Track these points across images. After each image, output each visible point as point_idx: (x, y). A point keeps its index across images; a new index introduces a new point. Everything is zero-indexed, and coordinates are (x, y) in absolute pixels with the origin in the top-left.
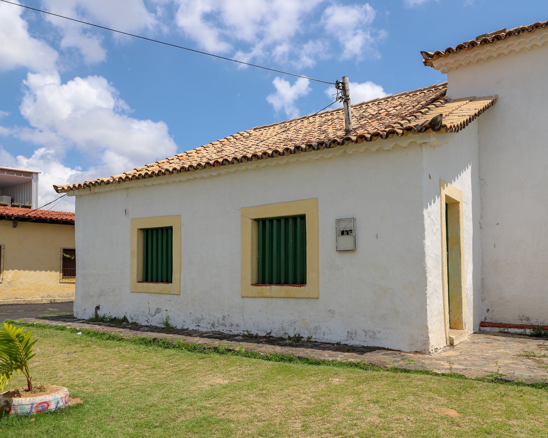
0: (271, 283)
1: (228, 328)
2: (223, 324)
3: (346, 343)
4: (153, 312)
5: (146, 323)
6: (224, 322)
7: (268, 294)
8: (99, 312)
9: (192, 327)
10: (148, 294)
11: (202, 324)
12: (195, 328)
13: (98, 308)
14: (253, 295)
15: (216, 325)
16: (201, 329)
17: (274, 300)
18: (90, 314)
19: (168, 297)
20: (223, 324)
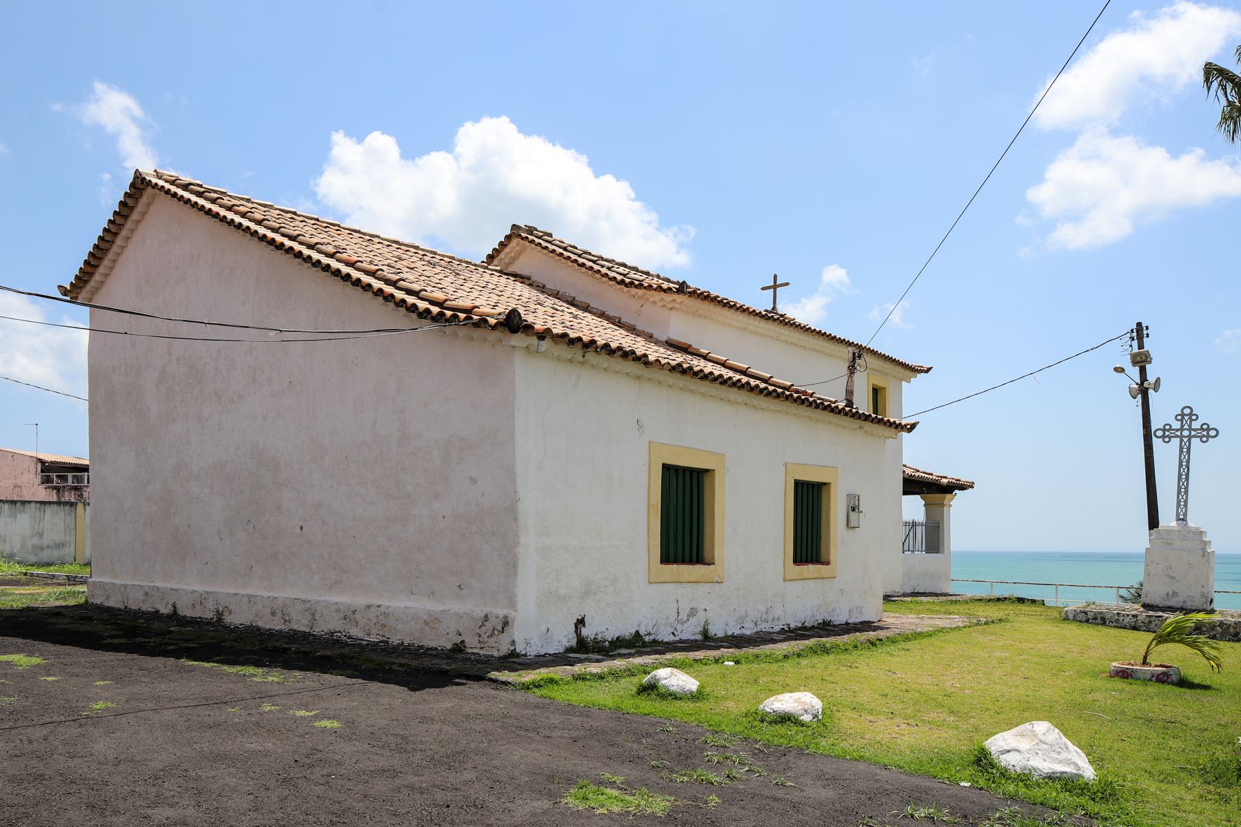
4: (683, 616)
5: (672, 638)
7: (806, 576)
8: (585, 632)
10: (676, 585)
13: (581, 622)
18: (563, 638)
19: (706, 588)
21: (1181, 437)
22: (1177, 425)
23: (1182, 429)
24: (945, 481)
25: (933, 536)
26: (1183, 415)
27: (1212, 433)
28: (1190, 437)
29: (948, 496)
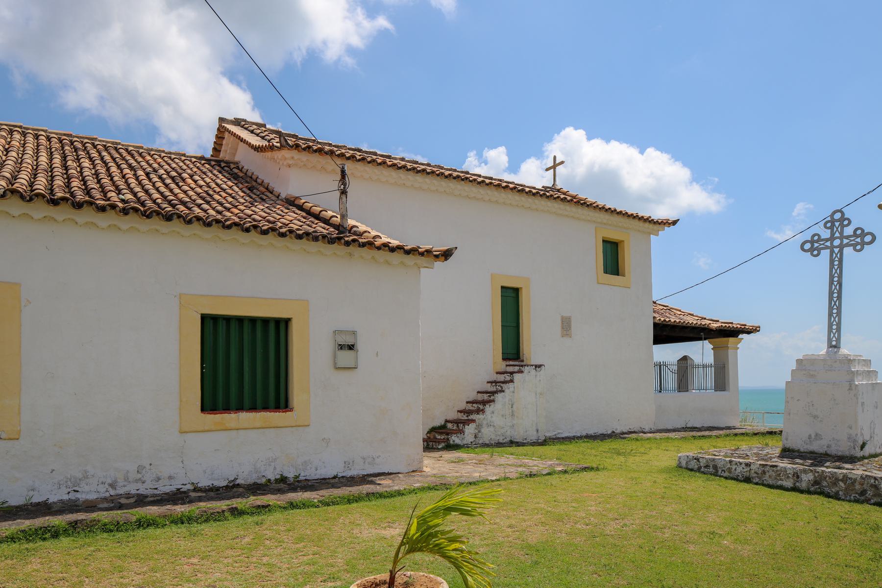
0: (240, 408)
1: (149, 484)
2: (137, 481)
3: (344, 475)
6: (139, 476)
9: (55, 496)
11: (84, 487)
12: (66, 497)
14: (207, 428)
15: (121, 482)
16: (82, 497)
17: (241, 432)
20: (137, 481)
21: (832, 248)
22: (826, 234)
23: (832, 238)
24: (714, 325)
25: (722, 378)
26: (833, 221)
27: (868, 239)
28: (841, 247)
29: (731, 339)
